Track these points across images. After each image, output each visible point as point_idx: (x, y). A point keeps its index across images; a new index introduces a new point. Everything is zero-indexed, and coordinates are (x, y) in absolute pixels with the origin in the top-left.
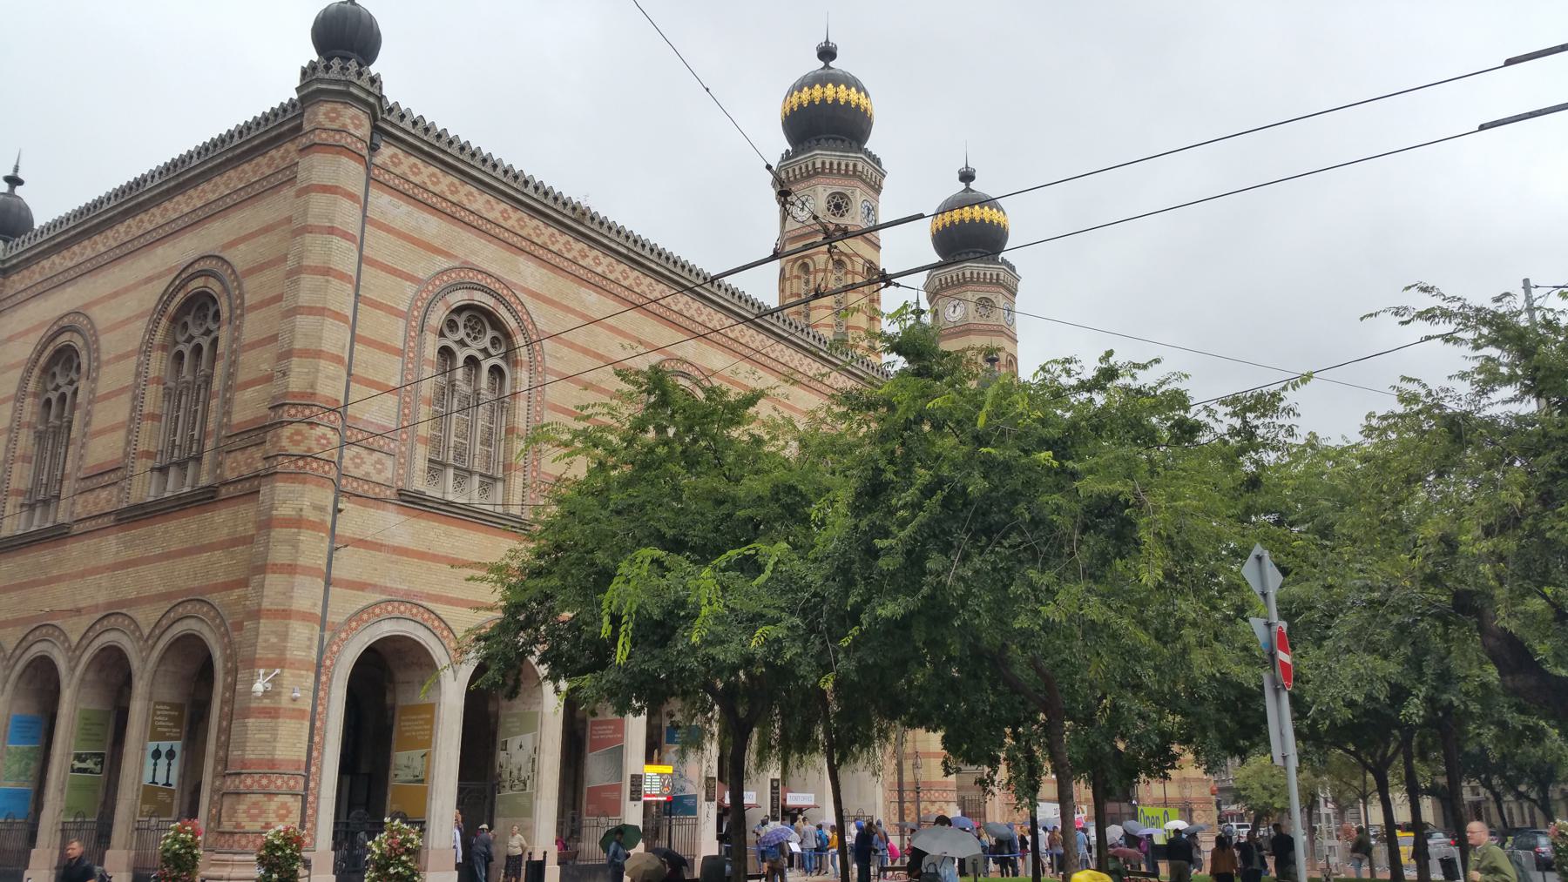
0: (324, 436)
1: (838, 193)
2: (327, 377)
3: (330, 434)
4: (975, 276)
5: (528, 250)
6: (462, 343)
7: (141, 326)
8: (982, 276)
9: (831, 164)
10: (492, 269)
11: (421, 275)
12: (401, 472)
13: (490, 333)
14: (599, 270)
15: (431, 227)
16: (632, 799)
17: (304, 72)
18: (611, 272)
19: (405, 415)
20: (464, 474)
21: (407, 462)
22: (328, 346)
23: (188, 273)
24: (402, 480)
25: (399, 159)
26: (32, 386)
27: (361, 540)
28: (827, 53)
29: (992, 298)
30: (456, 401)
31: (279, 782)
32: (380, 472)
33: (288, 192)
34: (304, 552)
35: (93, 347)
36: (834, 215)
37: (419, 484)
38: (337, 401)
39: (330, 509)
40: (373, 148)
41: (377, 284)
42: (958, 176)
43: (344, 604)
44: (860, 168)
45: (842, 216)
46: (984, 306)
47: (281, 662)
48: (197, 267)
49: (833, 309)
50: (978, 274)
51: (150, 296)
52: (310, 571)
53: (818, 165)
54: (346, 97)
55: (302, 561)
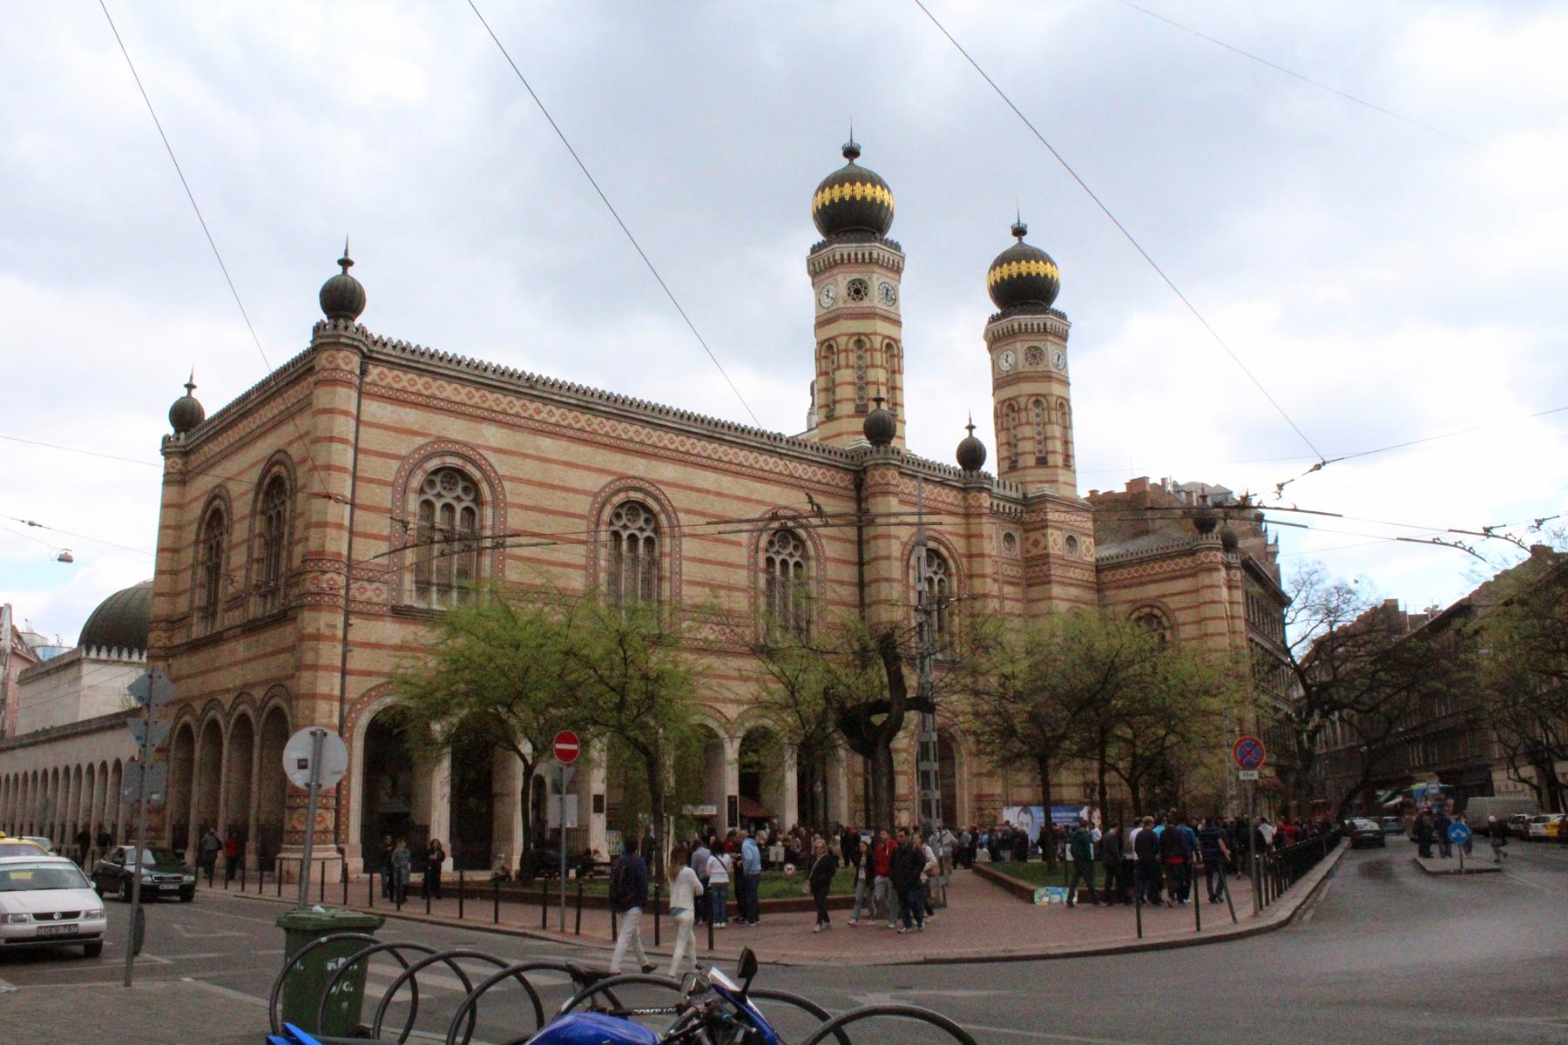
6: (439, 495)
7: (251, 496)
9: (849, 255)
10: (461, 438)
11: (403, 453)
14: (553, 420)
15: (411, 417)
16: (595, 811)
20: (445, 589)
21: (399, 588)
23: (271, 462)
26: (202, 537)
28: (851, 153)
32: (378, 596)
33: (308, 413)
35: (229, 509)
37: (410, 599)
38: (339, 554)
40: (363, 372)
41: (371, 467)
42: (1010, 231)
43: (356, 686)
44: (875, 256)
48: (274, 459)
49: (854, 384)
51: (254, 475)
53: (838, 257)
54: (338, 346)
55: (323, 661)
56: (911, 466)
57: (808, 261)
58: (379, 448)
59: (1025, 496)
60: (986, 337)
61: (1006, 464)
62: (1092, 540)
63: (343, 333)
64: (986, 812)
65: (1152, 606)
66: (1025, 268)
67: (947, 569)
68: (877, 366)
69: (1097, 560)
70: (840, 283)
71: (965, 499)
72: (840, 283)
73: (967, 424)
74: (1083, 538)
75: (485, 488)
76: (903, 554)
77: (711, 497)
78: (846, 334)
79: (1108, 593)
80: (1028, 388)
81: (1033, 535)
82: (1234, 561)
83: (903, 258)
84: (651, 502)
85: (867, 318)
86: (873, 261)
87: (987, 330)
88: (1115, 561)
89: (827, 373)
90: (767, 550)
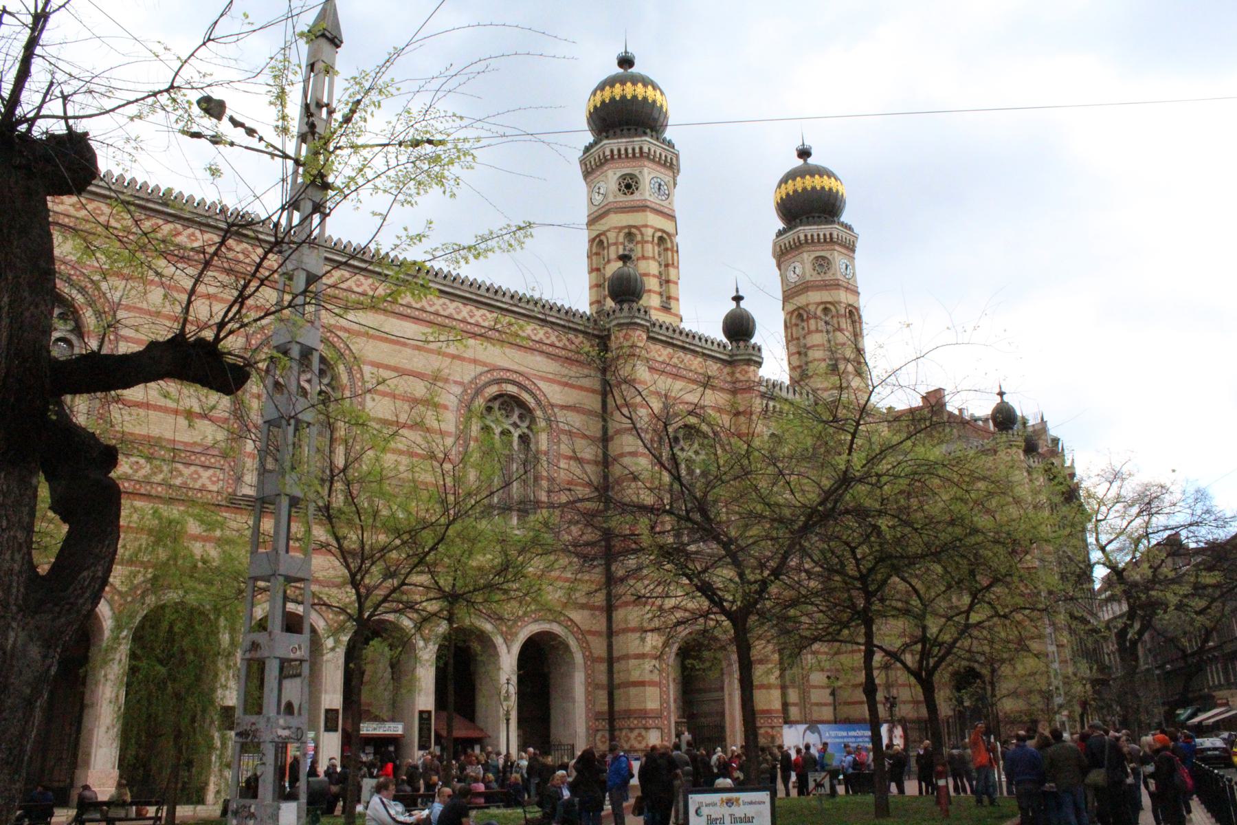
4: (809, 237)
8: (816, 237)
9: (619, 150)
42: (795, 154)
44: (646, 149)
45: (632, 193)
46: (821, 265)
50: (812, 236)
53: (608, 153)
61: (796, 375)
66: (809, 182)
70: (611, 178)
72: (611, 178)
73: (734, 294)
77: (409, 351)
78: (616, 228)
80: (815, 297)
83: (677, 156)
85: (637, 211)
86: (644, 155)
87: (775, 244)
89: (598, 270)
90: (482, 417)
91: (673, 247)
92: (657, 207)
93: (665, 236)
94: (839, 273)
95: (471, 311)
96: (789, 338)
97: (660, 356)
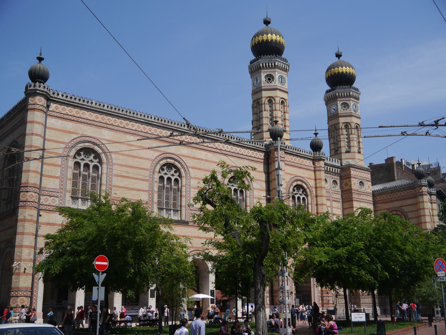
0: (32, 195)
1: (269, 74)
2: (32, 177)
3: (33, 194)
5: (106, 126)
6: (83, 159)
7: (3, 161)
11: (66, 141)
12: (61, 202)
13: (93, 155)
14: (134, 128)
15: (70, 126)
17: (26, 88)
18: (139, 128)
19: (62, 184)
21: (63, 198)
22: (31, 168)
24: (61, 204)
25: (58, 107)
27: (48, 223)
29: (348, 102)
30: (81, 178)
31: (21, 293)
32: (54, 202)
34: (26, 228)
36: (268, 82)
39: (36, 215)
40: (48, 106)
44: (277, 64)
45: (271, 82)
46: (345, 107)
47: (20, 260)
52: (28, 234)
53: (261, 65)
55: (26, 231)
56: (290, 150)
57: (249, 67)
58: (55, 139)
59: (341, 165)
60: (324, 100)
61: (333, 152)
62: (371, 183)
63: (38, 88)
64: (325, 298)
65: (397, 211)
67: (306, 192)
68: (277, 110)
69: (373, 192)
71: (314, 164)
73: (314, 132)
74: (367, 182)
75: (103, 156)
76: (287, 187)
77: (203, 162)
78: (264, 97)
79: (379, 205)
81: (345, 181)
82: (433, 191)
84: (177, 164)
86: (276, 67)
87: (325, 96)
88: (381, 192)
89: (257, 114)
91: (287, 105)
92: (281, 88)
93: (284, 100)
94: (352, 110)
95: (223, 145)
96: (330, 137)
97: (288, 159)
